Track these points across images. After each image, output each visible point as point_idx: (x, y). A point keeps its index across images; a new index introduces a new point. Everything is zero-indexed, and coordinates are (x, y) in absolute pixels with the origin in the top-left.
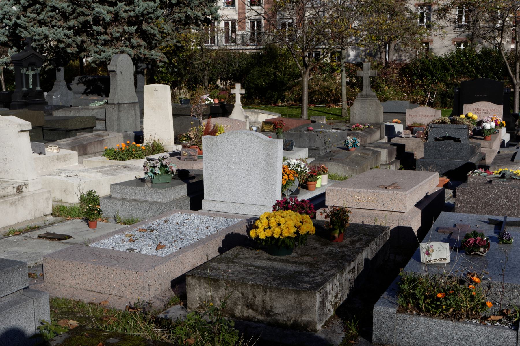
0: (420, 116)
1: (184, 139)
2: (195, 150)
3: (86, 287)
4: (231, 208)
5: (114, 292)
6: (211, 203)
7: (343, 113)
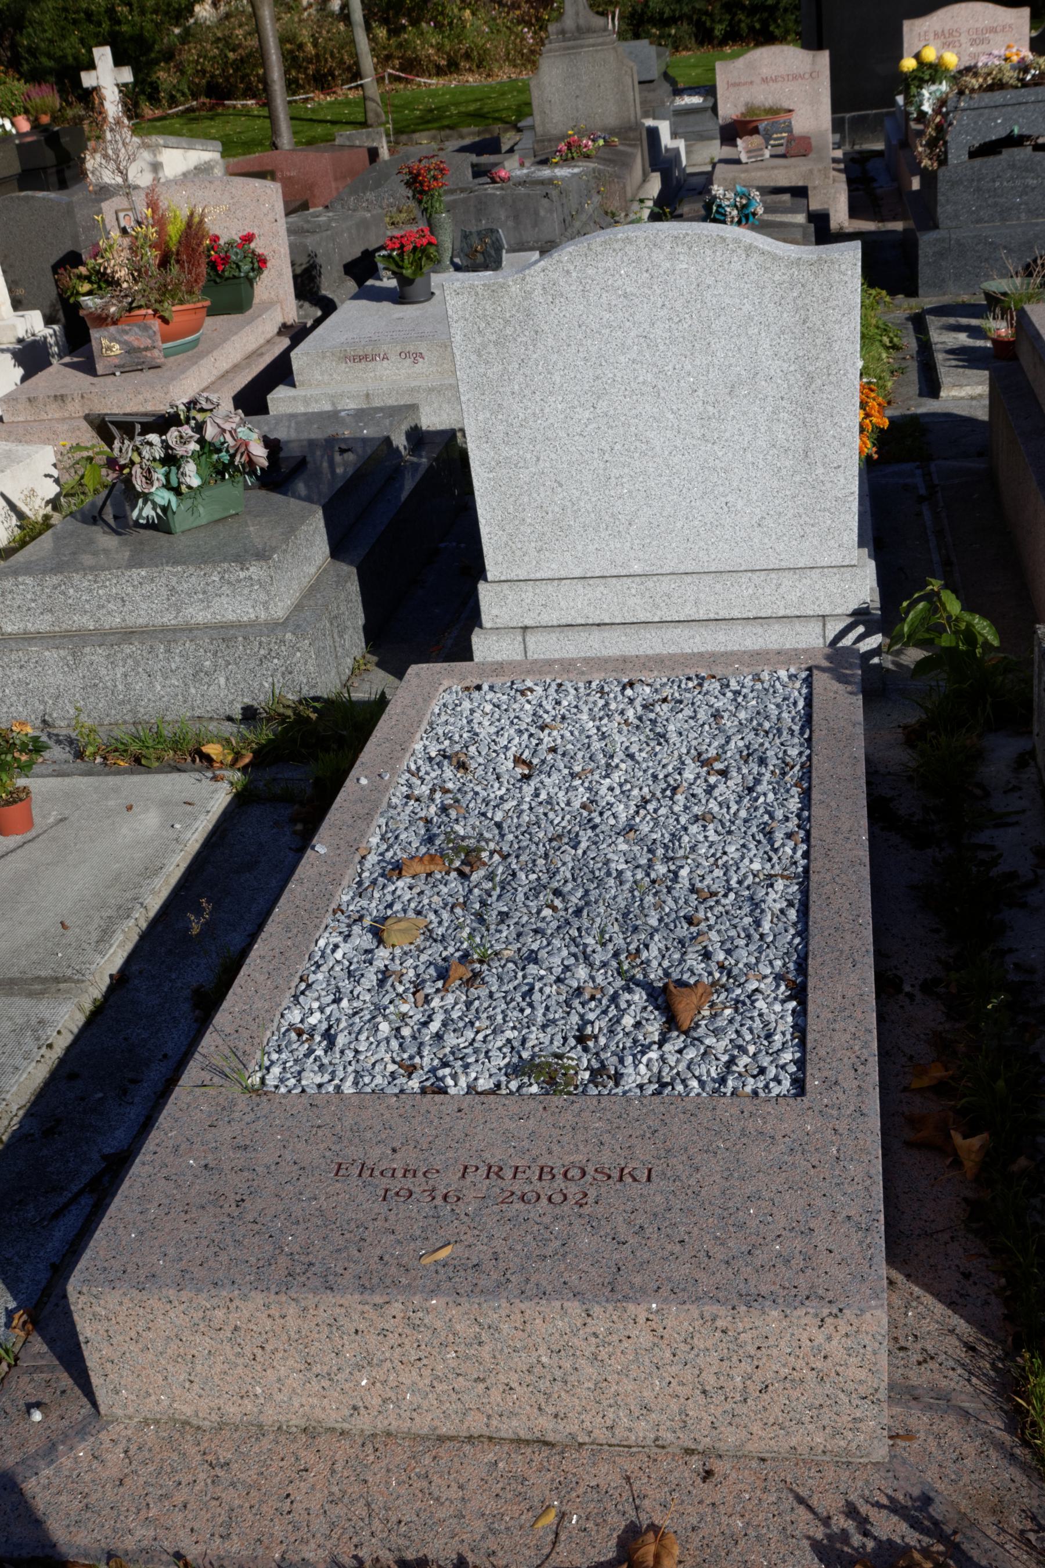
0: (765, 80)
1: (86, 287)
2: (146, 328)
3: (423, 1424)
4: (631, 602)
5: (643, 1431)
6: (528, 593)
7: (371, 115)
